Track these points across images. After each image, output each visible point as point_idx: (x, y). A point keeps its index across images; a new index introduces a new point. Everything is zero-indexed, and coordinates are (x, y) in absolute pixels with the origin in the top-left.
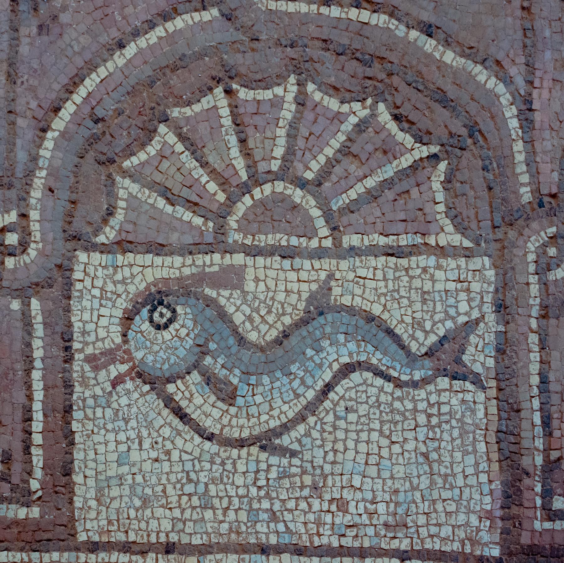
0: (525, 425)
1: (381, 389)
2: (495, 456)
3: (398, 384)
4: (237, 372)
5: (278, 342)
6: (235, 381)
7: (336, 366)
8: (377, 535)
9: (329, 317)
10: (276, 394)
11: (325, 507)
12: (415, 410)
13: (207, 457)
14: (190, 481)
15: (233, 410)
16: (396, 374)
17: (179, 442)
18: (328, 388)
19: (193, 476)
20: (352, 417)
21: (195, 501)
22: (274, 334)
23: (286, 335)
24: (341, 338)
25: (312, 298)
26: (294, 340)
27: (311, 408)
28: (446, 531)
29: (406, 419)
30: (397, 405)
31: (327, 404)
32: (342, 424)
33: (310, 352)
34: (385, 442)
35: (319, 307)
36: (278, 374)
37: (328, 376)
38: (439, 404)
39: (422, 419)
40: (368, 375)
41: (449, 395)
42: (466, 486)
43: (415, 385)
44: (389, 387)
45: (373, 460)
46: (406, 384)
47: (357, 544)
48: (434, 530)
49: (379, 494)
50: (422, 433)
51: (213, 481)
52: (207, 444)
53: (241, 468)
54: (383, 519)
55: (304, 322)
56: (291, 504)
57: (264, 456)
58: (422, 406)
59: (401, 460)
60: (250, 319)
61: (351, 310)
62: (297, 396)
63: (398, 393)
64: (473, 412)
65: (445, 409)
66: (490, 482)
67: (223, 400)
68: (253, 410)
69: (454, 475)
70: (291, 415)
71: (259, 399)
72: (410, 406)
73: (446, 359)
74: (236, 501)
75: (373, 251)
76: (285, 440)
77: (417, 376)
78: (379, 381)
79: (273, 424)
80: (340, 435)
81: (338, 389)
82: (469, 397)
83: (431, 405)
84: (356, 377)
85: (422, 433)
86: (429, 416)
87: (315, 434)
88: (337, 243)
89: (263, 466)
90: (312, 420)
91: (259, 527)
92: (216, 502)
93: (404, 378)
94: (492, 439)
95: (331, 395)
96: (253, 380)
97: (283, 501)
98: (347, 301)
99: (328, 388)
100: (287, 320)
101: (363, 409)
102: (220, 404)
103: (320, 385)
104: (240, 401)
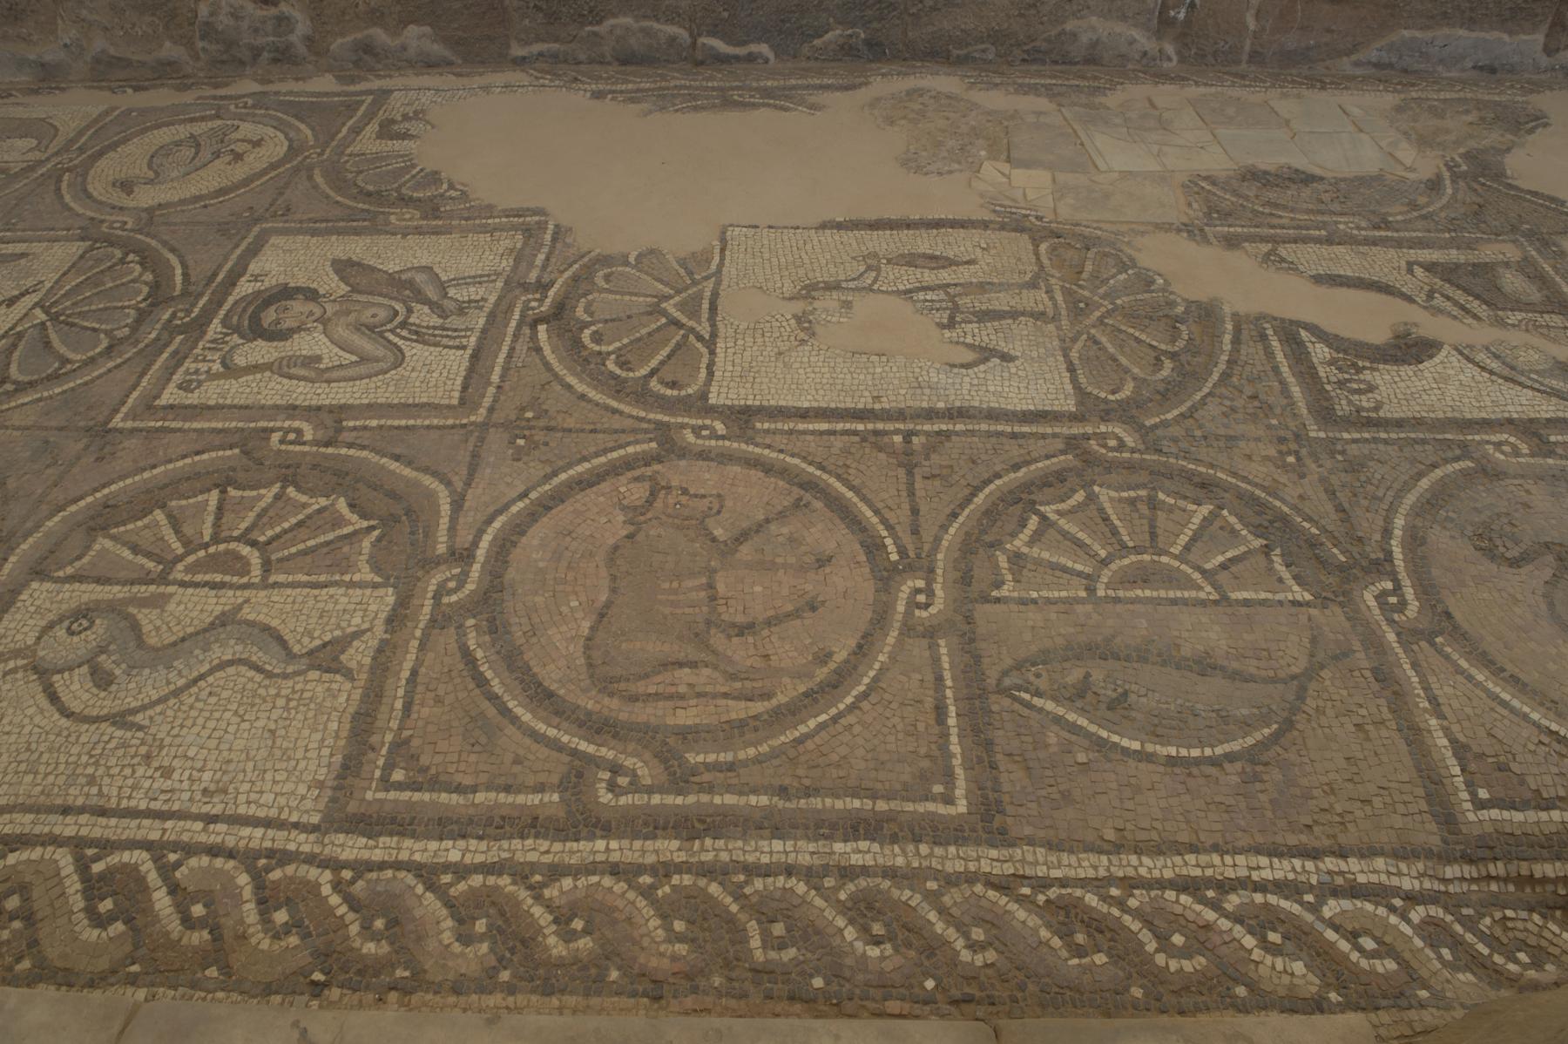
0: (384, 709)
1: (251, 680)
2: (344, 734)
3: (269, 675)
4: (124, 666)
5: (174, 644)
6: (117, 672)
7: (216, 662)
8: (191, 799)
9: (229, 628)
10: (150, 682)
11: (149, 773)
12: (278, 695)
13: (56, 730)
14: (28, 749)
15: (103, 694)
16: (268, 667)
17: (37, 720)
18: (202, 677)
19: (34, 746)
20: (213, 700)
21: (23, 767)
22: (174, 638)
23: (183, 640)
24: (232, 642)
25: (223, 613)
26: (187, 644)
27: (176, 693)
28: (268, 798)
29: (265, 701)
30: (262, 691)
31: (194, 690)
32: (200, 705)
33: (197, 652)
34: (236, 720)
35: (223, 621)
36: (160, 668)
37: (205, 668)
38: (303, 691)
39: (281, 702)
40: (243, 669)
41: (315, 684)
42: (305, 758)
43: (285, 676)
44: (258, 677)
45: (217, 734)
46: (277, 675)
47: (165, 808)
48: (253, 796)
49: (210, 765)
50: (275, 714)
51: (50, 750)
52: (64, 720)
53: (83, 739)
54: (203, 785)
55: (205, 630)
56: (116, 771)
57: (110, 730)
58: (284, 692)
59: (246, 735)
60: (158, 629)
61: (251, 624)
62: (168, 683)
63: (267, 682)
64: (335, 697)
65: (306, 695)
66: (332, 755)
67: (98, 686)
68: (122, 695)
69: (295, 749)
70: (154, 698)
71: (131, 686)
72: (273, 691)
73: (327, 658)
74: (62, 767)
75: (293, 585)
76: (139, 718)
77: (290, 669)
78: (252, 673)
79: (133, 705)
80: (194, 713)
81: (210, 679)
82: (335, 686)
83: (294, 692)
84: (231, 670)
85: (275, 714)
86: (289, 700)
87: (170, 713)
88: (264, 578)
89: (106, 738)
90: (172, 701)
91: (72, 791)
92: (42, 769)
93: (276, 671)
94: (347, 718)
95: (202, 683)
96: (134, 672)
97: (109, 768)
98: (251, 617)
99: (202, 677)
100: (190, 630)
101: (225, 694)
102: (95, 690)
103: (195, 674)
104: (114, 688)
